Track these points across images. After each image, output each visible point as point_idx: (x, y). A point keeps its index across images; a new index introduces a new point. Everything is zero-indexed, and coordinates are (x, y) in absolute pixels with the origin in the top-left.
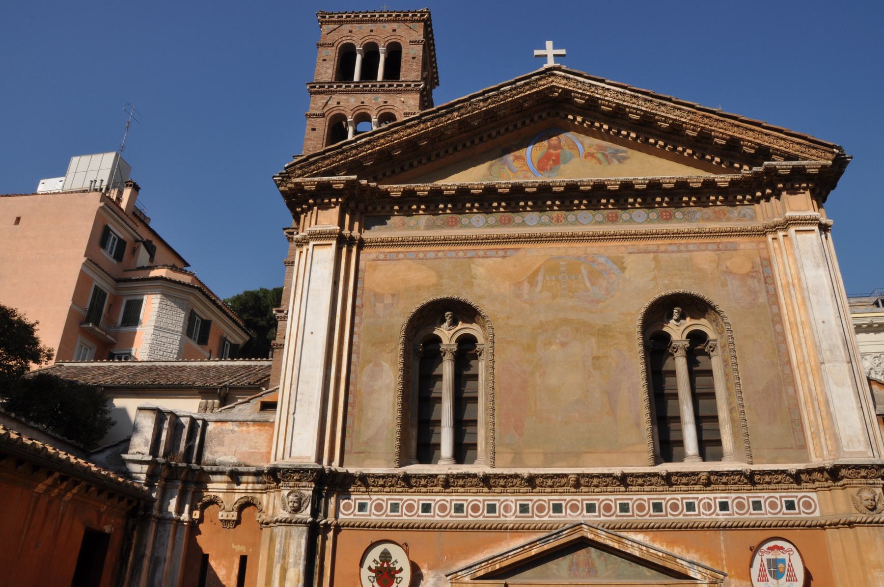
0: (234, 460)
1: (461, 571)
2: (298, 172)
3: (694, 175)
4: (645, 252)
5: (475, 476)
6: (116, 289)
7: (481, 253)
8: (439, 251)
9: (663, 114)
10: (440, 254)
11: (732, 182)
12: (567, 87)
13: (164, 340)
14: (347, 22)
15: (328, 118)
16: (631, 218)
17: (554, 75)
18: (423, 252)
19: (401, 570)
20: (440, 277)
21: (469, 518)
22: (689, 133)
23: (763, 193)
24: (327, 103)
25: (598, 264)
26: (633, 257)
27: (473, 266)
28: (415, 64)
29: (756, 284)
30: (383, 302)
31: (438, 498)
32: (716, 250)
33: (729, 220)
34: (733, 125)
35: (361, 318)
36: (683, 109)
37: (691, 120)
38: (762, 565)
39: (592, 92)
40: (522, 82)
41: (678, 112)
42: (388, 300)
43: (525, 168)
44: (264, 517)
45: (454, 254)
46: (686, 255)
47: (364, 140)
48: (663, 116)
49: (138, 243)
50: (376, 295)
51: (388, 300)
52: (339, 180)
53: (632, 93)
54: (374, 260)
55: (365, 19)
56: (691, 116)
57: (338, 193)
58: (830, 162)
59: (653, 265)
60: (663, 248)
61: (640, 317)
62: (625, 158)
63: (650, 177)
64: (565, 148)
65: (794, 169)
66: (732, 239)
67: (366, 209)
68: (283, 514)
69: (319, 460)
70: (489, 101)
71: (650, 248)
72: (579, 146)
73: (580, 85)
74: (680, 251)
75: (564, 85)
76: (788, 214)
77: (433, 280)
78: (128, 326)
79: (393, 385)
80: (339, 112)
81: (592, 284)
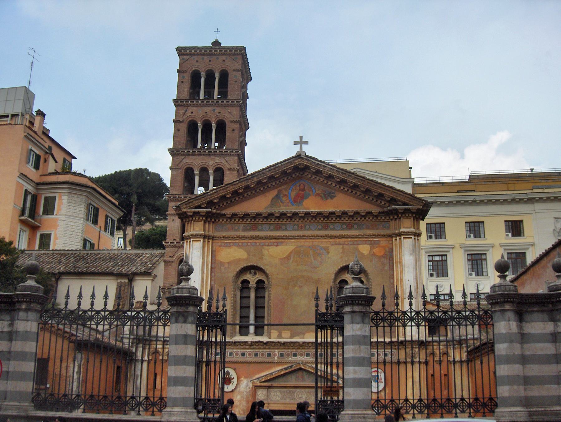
1: (256, 379)
2: (185, 206)
5: (263, 342)
6: (37, 189)
7: (267, 244)
8: (248, 242)
10: (249, 244)
12: (307, 164)
13: (72, 224)
14: (195, 55)
15: (187, 123)
16: (334, 227)
18: (242, 242)
19: (233, 378)
21: (260, 359)
23: (394, 217)
24: (185, 113)
26: (333, 247)
27: (263, 250)
28: (236, 86)
29: (385, 261)
30: (224, 266)
31: (248, 350)
32: (370, 244)
33: (377, 229)
34: (381, 187)
40: (287, 162)
41: (357, 180)
42: (226, 265)
43: (288, 201)
45: (254, 244)
46: (356, 246)
47: (214, 191)
49: (48, 155)
51: (226, 265)
52: (203, 211)
54: (220, 246)
55: (205, 53)
56: (363, 182)
58: (421, 207)
59: (341, 251)
60: (346, 243)
61: (333, 275)
62: (334, 197)
63: (342, 210)
64: (307, 191)
70: (271, 171)
71: (341, 243)
72: (313, 189)
74: (354, 244)
75: (306, 163)
76: (401, 230)
78: (47, 215)
80: (192, 119)
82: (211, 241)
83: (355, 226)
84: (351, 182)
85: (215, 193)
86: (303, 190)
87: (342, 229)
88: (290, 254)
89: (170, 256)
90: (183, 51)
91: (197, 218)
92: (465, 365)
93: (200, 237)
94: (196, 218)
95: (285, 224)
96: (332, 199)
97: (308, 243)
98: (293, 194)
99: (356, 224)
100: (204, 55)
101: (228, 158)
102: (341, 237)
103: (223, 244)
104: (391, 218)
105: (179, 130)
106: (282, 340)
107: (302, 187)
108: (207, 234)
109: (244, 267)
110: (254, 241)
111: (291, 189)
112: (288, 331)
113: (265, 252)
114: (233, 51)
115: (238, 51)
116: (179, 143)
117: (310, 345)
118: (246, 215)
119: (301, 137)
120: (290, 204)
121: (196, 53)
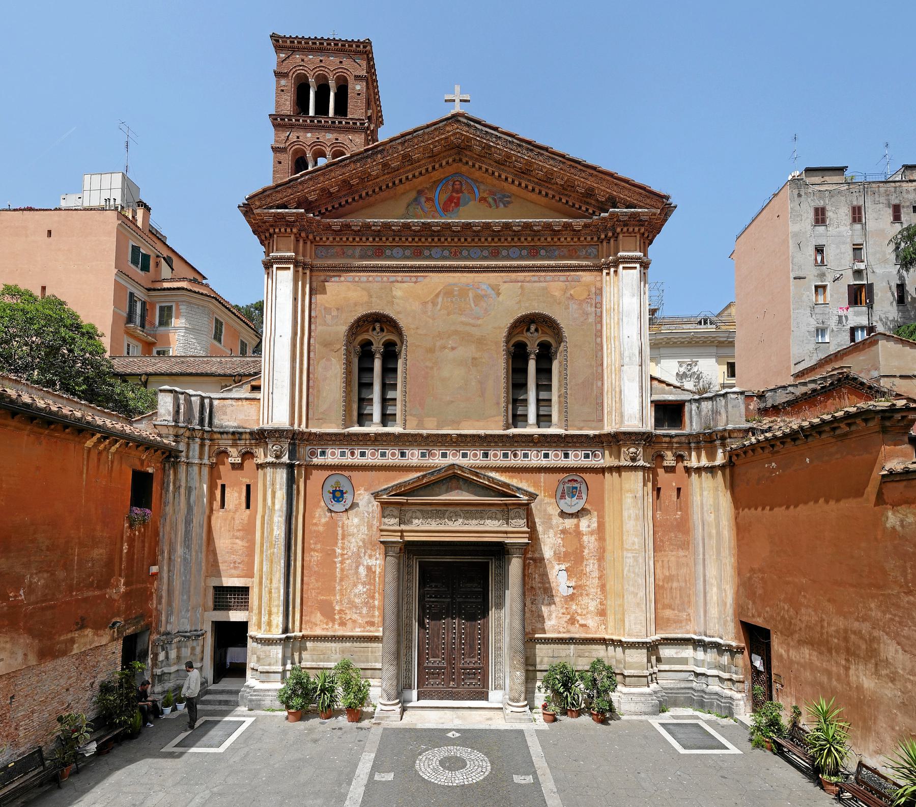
0: (235, 424)
4: (515, 282)
8: (369, 276)
9: (540, 163)
10: (371, 279)
11: (586, 226)
12: (468, 134)
17: (459, 121)
20: (371, 296)
22: (559, 181)
23: (606, 236)
25: (482, 290)
26: (506, 285)
35: (316, 327)
36: (556, 159)
37: (561, 169)
38: (564, 490)
39: (488, 140)
40: (433, 128)
41: (551, 162)
44: (259, 461)
45: (380, 279)
48: (540, 165)
50: (325, 308)
51: (335, 313)
53: (518, 142)
57: (290, 224)
60: (528, 279)
62: (509, 203)
66: (577, 273)
67: (315, 239)
68: (270, 459)
69: (292, 424)
70: (406, 144)
71: (519, 279)
72: (476, 190)
73: (478, 133)
76: (620, 254)
77: (366, 299)
79: (339, 375)
81: (476, 306)
82: (308, 272)
83: (543, 252)
86: (460, 191)
91: (283, 230)
94: (280, 230)
95: (429, 248)
99: (543, 249)
104: (603, 236)
106: (425, 432)
107: (457, 186)
108: (300, 258)
109: (363, 316)
110: (379, 274)
111: (439, 189)
112: (434, 417)
117: (468, 440)
118: (368, 226)
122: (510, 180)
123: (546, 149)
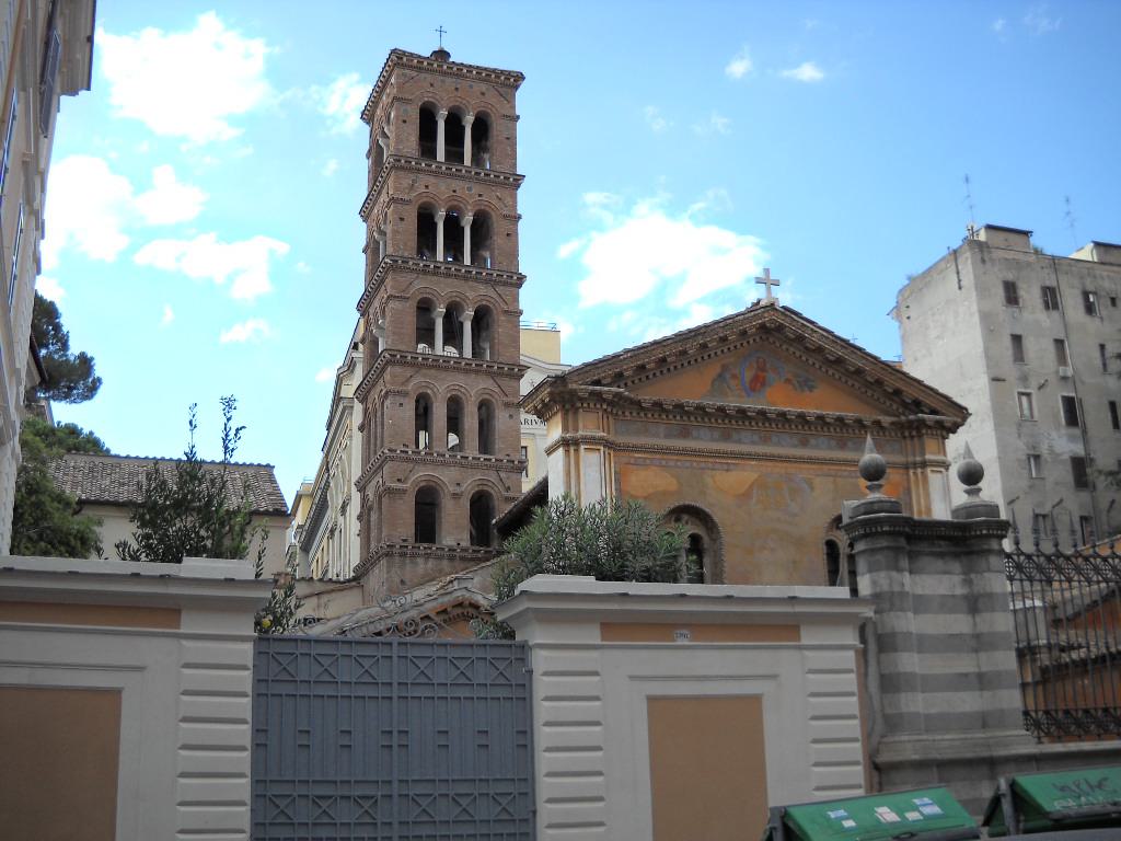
3: (868, 416)
8: (677, 460)
11: (893, 423)
34: (901, 379)
41: (864, 361)
45: (688, 464)
46: (854, 480)
56: (873, 366)
65: (937, 422)
81: (792, 500)
84: (853, 365)
85: (631, 357)
86: (762, 369)
87: (830, 448)
88: (751, 487)
89: (399, 480)
90: (405, 59)
92: (1040, 688)
93: (600, 444)
96: (811, 391)
97: (780, 468)
98: (748, 375)
100: (445, 74)
101: (500, 289)
102: (831, 462)
103: (632, 461)
104: (907, 434)
105: (402, 219)
113: (709, 480)
114: (502, 78)
115: (512, 80)
116: (405, 244)
119: (767, 271)
120: (744, 394)
121: (430, 67)
122: (817, 366)
123: (860, 349)
